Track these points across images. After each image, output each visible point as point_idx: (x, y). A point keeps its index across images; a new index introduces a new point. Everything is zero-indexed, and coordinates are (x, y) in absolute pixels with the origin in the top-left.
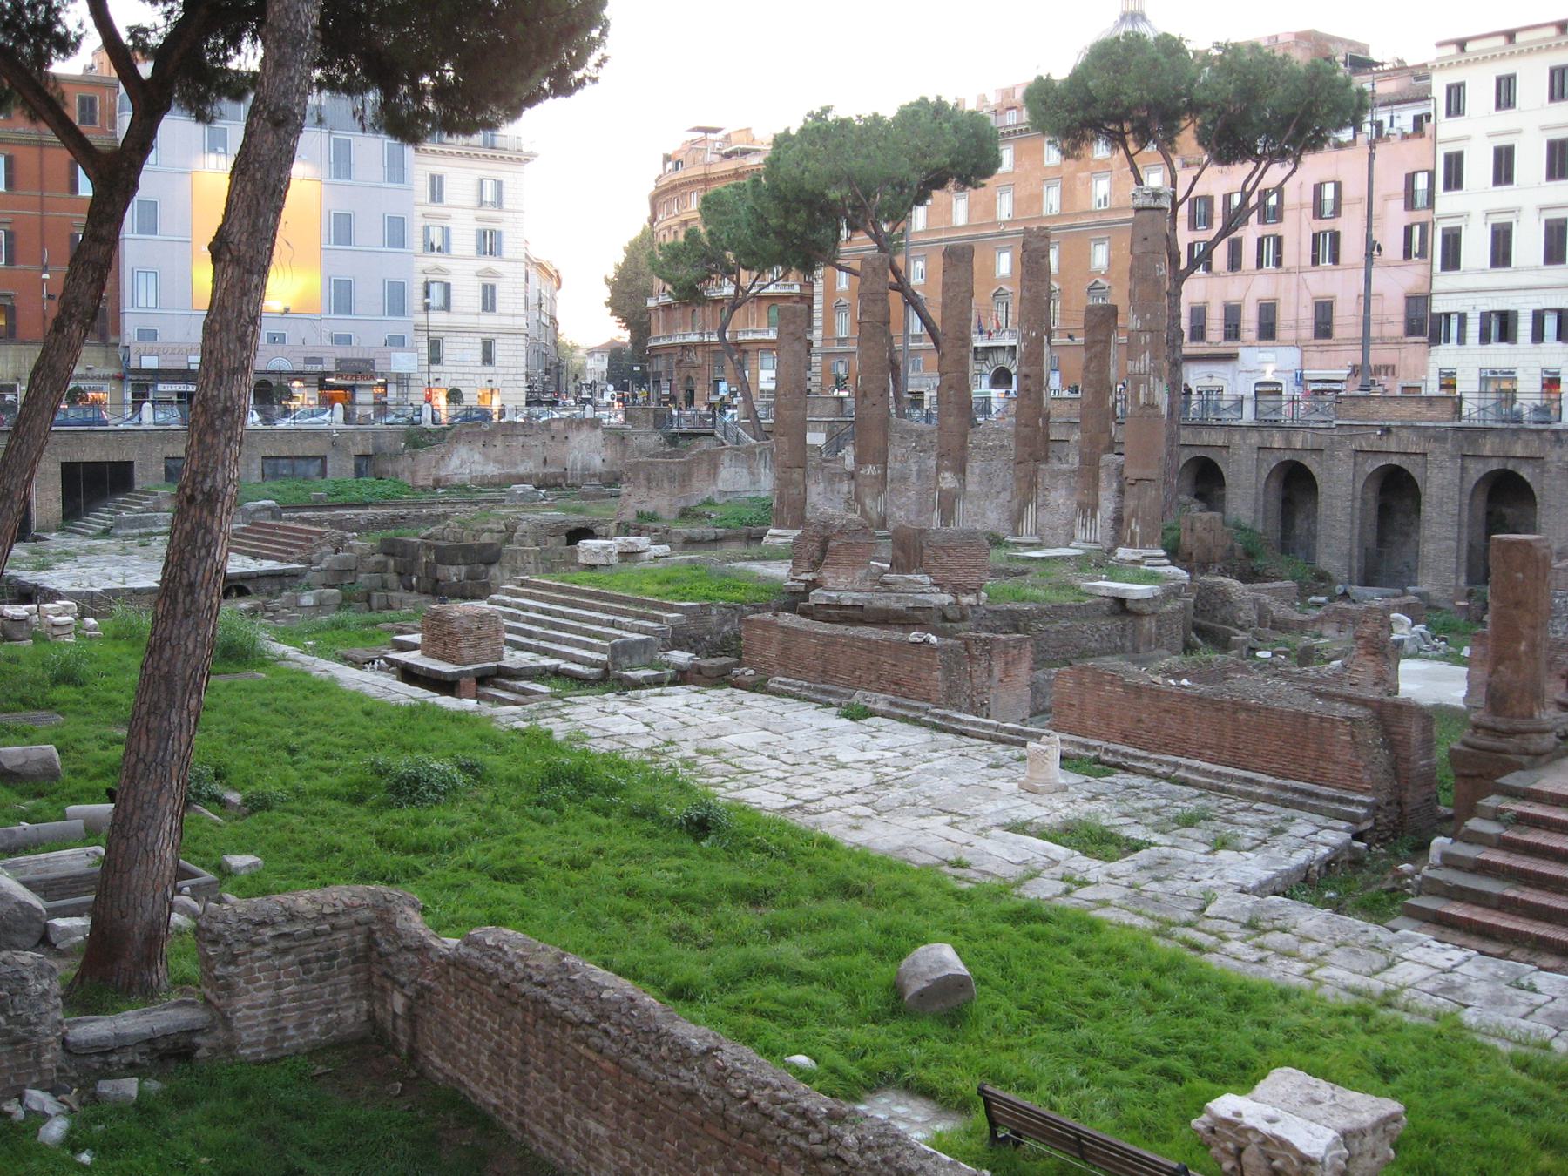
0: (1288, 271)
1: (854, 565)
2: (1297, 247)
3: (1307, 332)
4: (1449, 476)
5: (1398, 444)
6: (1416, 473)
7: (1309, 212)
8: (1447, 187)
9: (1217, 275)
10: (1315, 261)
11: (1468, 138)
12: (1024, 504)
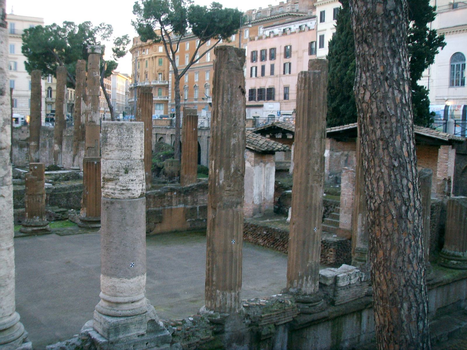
0: (277, 76)
2: (279, 69)
3: (282, 97)
7: (283, 56)
8: (320, 47)
9: (258, 78)
10: (284, 73)
11: (326, 30)
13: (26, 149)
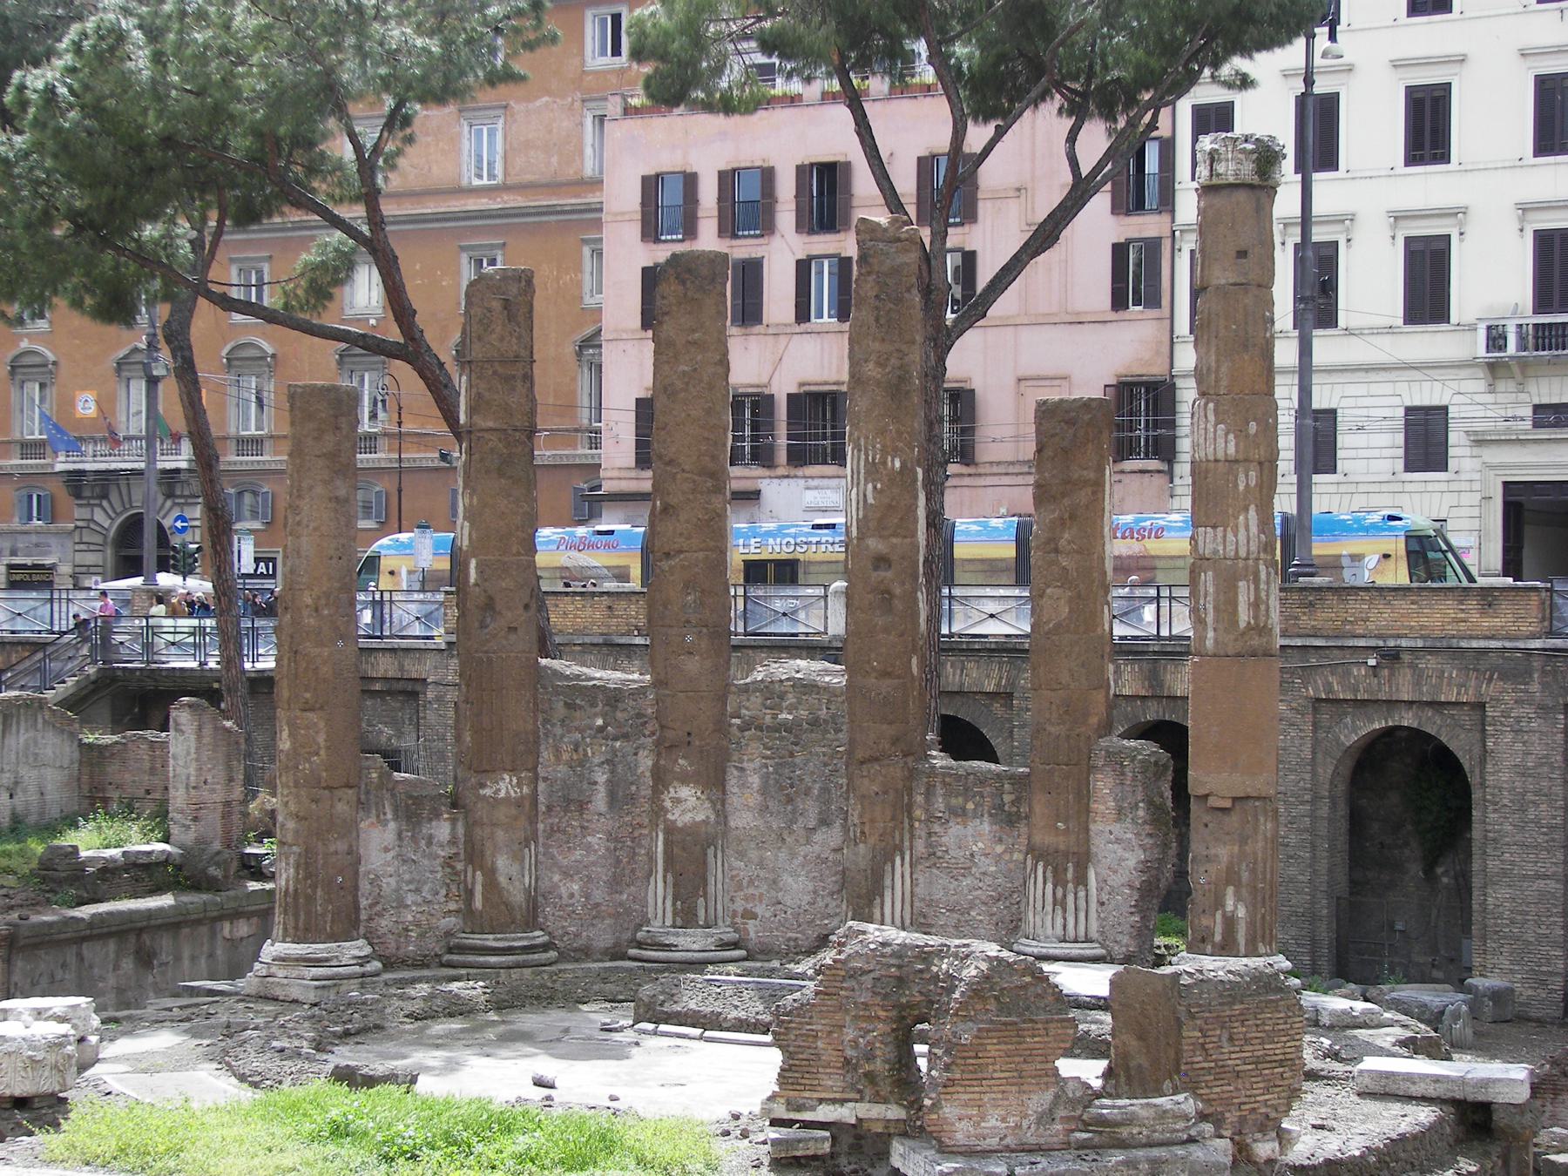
1: (1020, 1080)
4: (1538, 749)
5: (1417, 684)
6: (1460, 744)
12: (885, 855)
13: (442, 830)
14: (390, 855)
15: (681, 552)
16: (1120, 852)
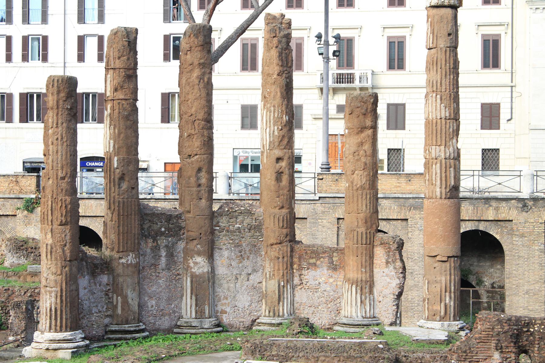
14: (87, 290)
15: (196, 155)
16: (388, 280)
